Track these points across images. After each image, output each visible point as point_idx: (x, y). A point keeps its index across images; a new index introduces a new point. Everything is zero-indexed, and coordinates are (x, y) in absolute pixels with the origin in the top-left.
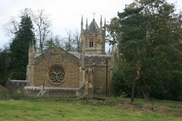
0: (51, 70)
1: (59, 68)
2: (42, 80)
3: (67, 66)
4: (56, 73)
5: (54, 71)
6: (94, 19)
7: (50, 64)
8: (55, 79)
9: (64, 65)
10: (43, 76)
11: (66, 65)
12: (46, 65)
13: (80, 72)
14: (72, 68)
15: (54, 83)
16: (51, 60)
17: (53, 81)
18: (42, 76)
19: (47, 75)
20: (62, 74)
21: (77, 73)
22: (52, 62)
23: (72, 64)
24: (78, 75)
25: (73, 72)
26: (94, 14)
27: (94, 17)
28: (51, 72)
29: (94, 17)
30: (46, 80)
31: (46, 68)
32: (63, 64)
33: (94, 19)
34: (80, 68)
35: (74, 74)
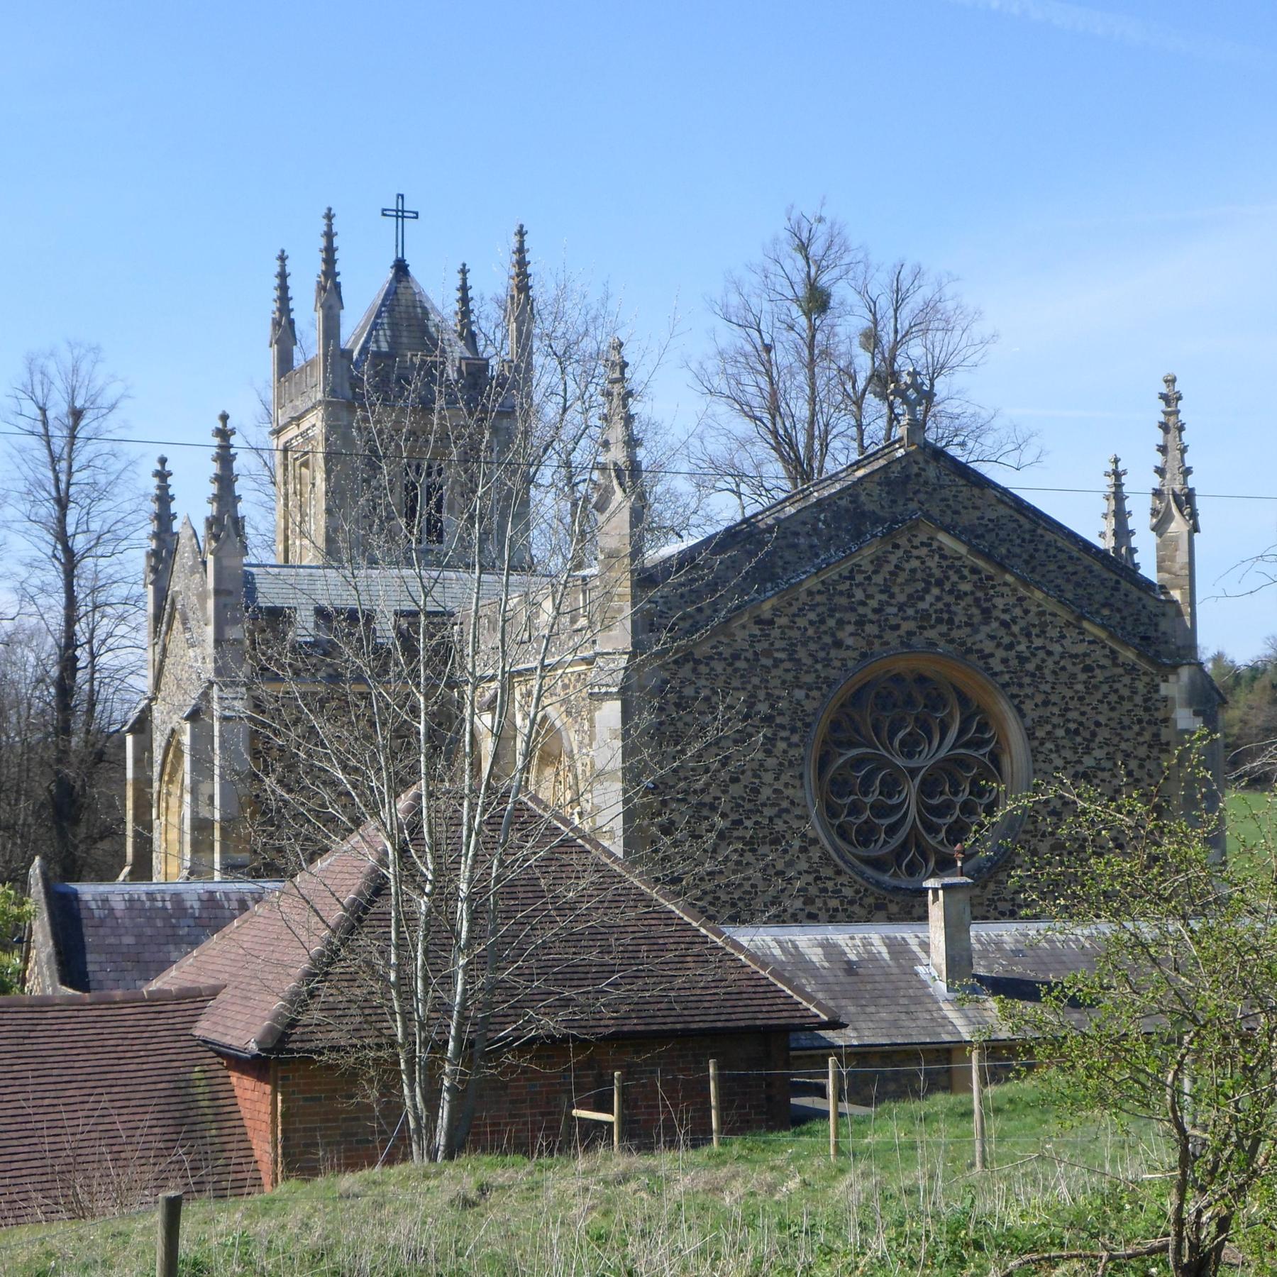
0: (835, 726)
1: (935, 702)
2: (751, 845)
3: (1030, 667)
4: (900, 762)
5: (876, 729)
6: (401, 268)
7: (838, 644)
8: (892, 830)
9: (1000, 653)
10: (766, 792)
11: (1022, 659)
12: (802, 654)
13: (1165, 735)
14: (1090, 688)
15: (886, 878)
16: (851, 596)
17: (874, 851)
18: (756, 791)
19: (810, 773)
20: (962, 763)
21: (1142, 751)
22: (861, 623)
23: (1081, 649)
24: (1149, 765)
25: (1103, 734)
26: (400, 214)
27: (400, 242)
28: (839, 744)
29: (400, 242)
30: (797, 843)
31: (799, 694)
32: (989, 647)
33: (401, 268)
34: (1164, 689)
35: (1110, 757)
